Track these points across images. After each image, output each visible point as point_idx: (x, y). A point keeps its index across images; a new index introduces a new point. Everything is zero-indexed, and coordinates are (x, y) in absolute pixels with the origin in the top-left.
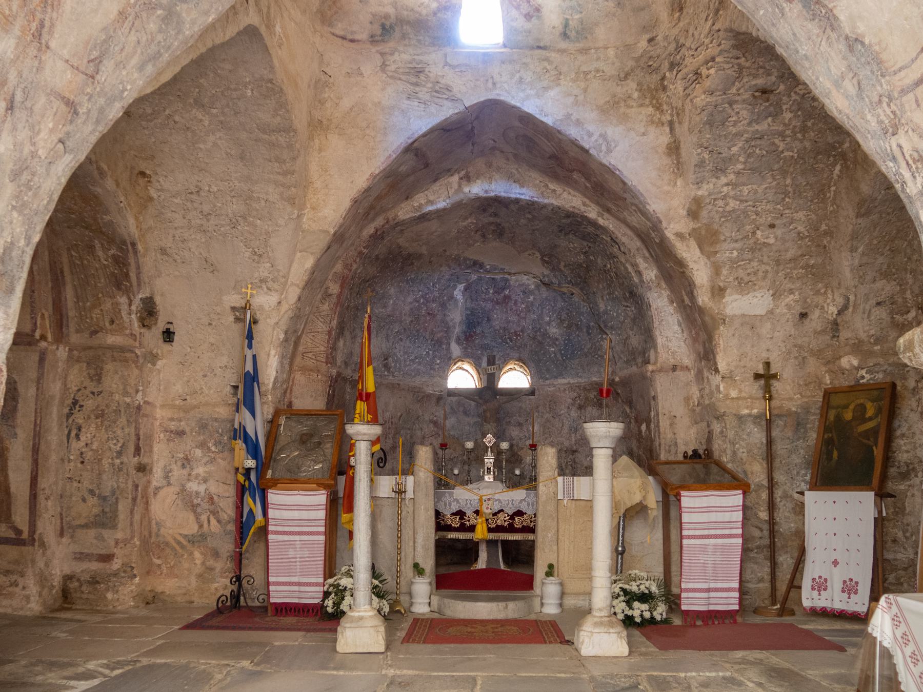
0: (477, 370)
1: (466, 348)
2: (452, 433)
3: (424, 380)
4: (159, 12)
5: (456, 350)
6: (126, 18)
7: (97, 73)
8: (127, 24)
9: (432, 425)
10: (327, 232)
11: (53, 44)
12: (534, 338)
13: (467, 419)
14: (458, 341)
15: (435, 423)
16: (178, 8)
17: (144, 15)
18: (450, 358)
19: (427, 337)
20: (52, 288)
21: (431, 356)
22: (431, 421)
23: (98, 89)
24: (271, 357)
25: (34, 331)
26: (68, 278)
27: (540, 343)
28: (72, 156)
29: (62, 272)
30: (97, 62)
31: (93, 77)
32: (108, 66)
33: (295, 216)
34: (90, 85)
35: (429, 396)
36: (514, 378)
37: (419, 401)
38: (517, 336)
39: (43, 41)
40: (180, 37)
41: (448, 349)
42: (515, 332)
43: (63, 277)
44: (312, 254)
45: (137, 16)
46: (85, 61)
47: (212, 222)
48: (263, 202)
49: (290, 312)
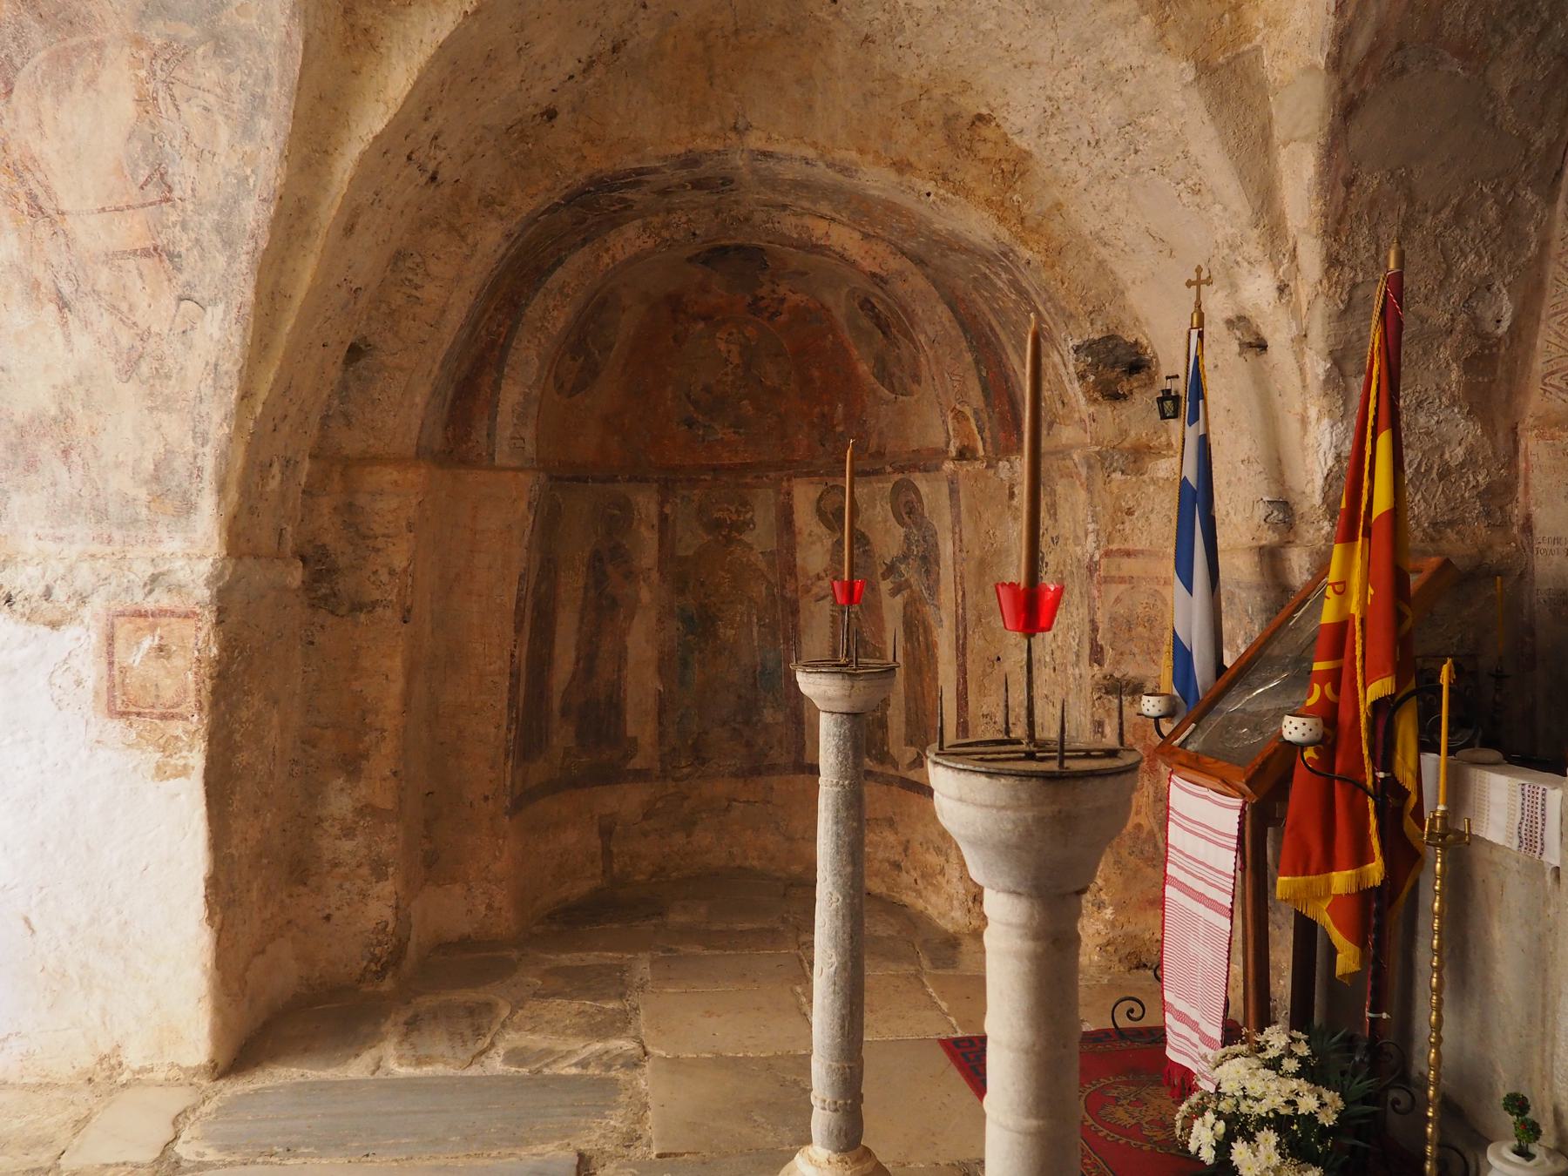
4: (200, 51)
6: (155, 99)
7: (170, 190)
8: (164, 102)
10: (1313, 68)
11: (65, 206)
16: (224, 22)
17: (181, 73)
20: (977, 362)
23: (190, 207)
24: (1312, 428)
25: (948, 444)
26: (1003, 337)
28: (221, 307)
29: (992, 329)
30: (160, 176)
31: (168, 200)
32: (183, 173)
33: (1190, 75)
34: (171, 210)
39: (50, 212)
40: (270, 50)
43: (997, 338)
44: (1306, 139)
45: (169, 85)
46: (135, 190)
47: (1109, 156)
48: (1129, 75)
49: (1321, 301)
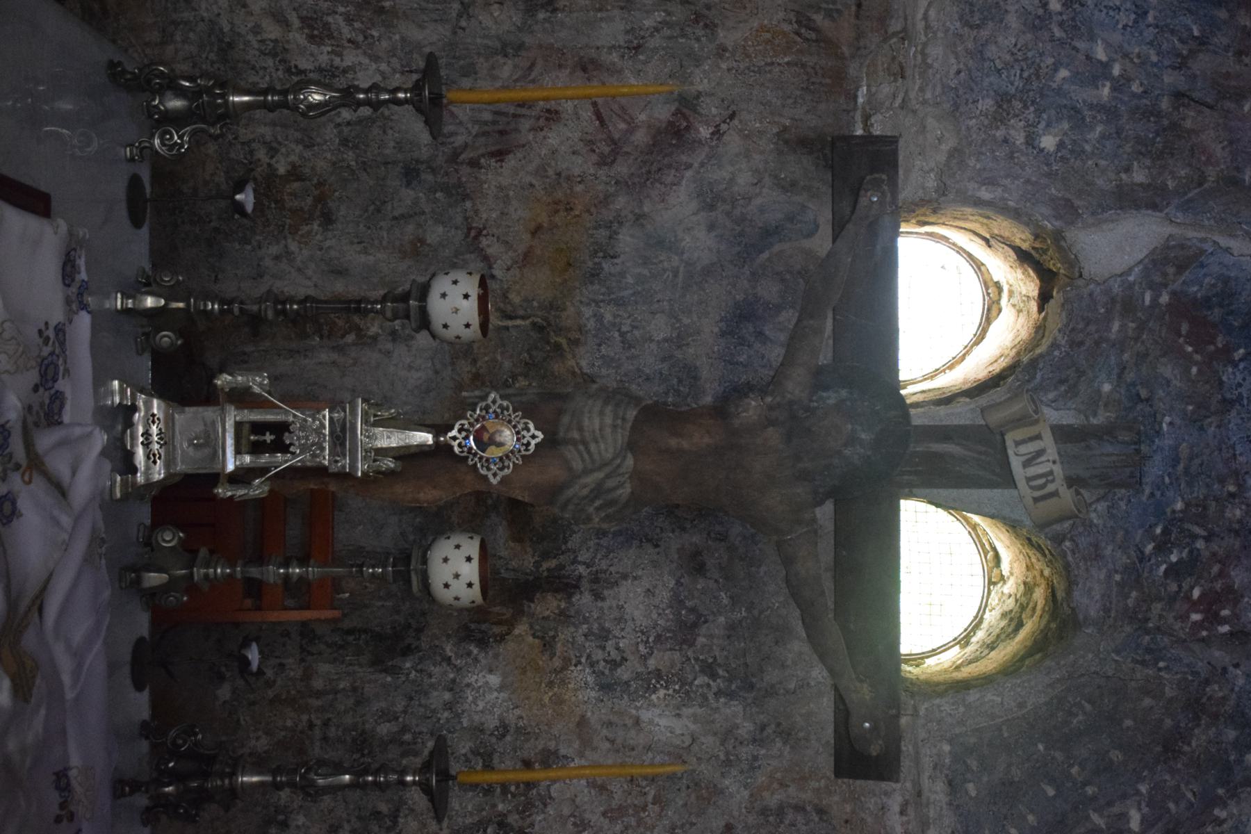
0: (993, 382)
1: (1128, 306)
2: (627, 240)
3: (936, 52)
5: (1116, 247)
9: (663, 113)
12: (1196, 706)
13: (709, 327)
14: (1169, 260)
15: (675, 135)
18: (1068, 211)
19: (1203, 63)
21: (1082, 95)
22: (687, 105)
27: (1171, 746)
35: (838, 83)
36: (950, 584)
37: (803, 21)
38: (1210, 604)
41: (1126, 200)
42: (1231, 595)
